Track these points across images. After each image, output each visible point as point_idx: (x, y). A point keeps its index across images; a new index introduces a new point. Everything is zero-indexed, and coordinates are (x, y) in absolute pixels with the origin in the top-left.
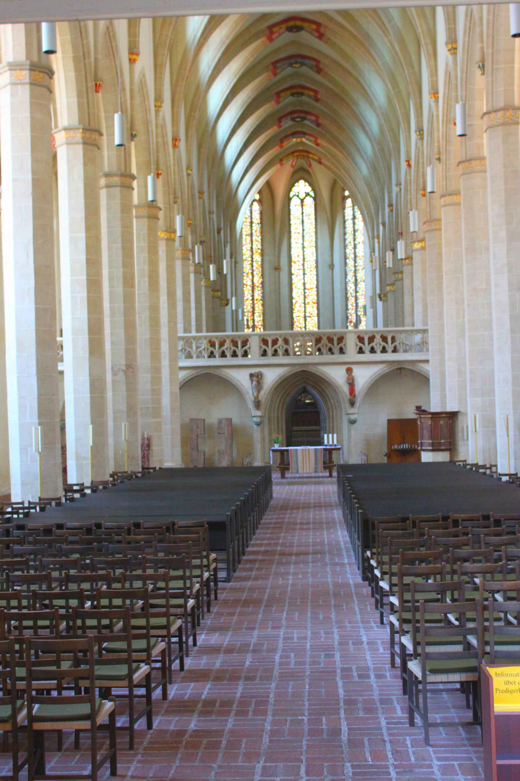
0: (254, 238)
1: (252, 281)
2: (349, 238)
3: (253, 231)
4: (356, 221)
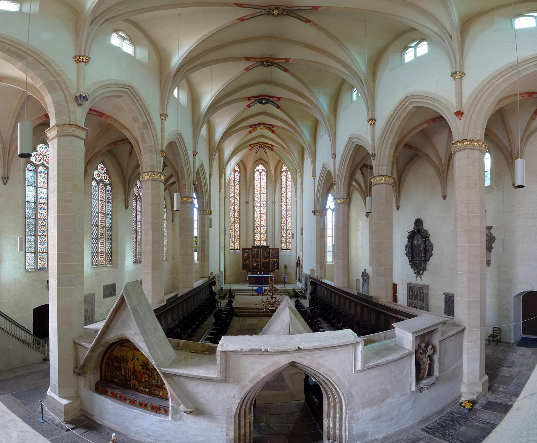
0: (236, 188)
1: (234, 208)
2: (284, 190)
3: (236, 185)
4: (288, 181)
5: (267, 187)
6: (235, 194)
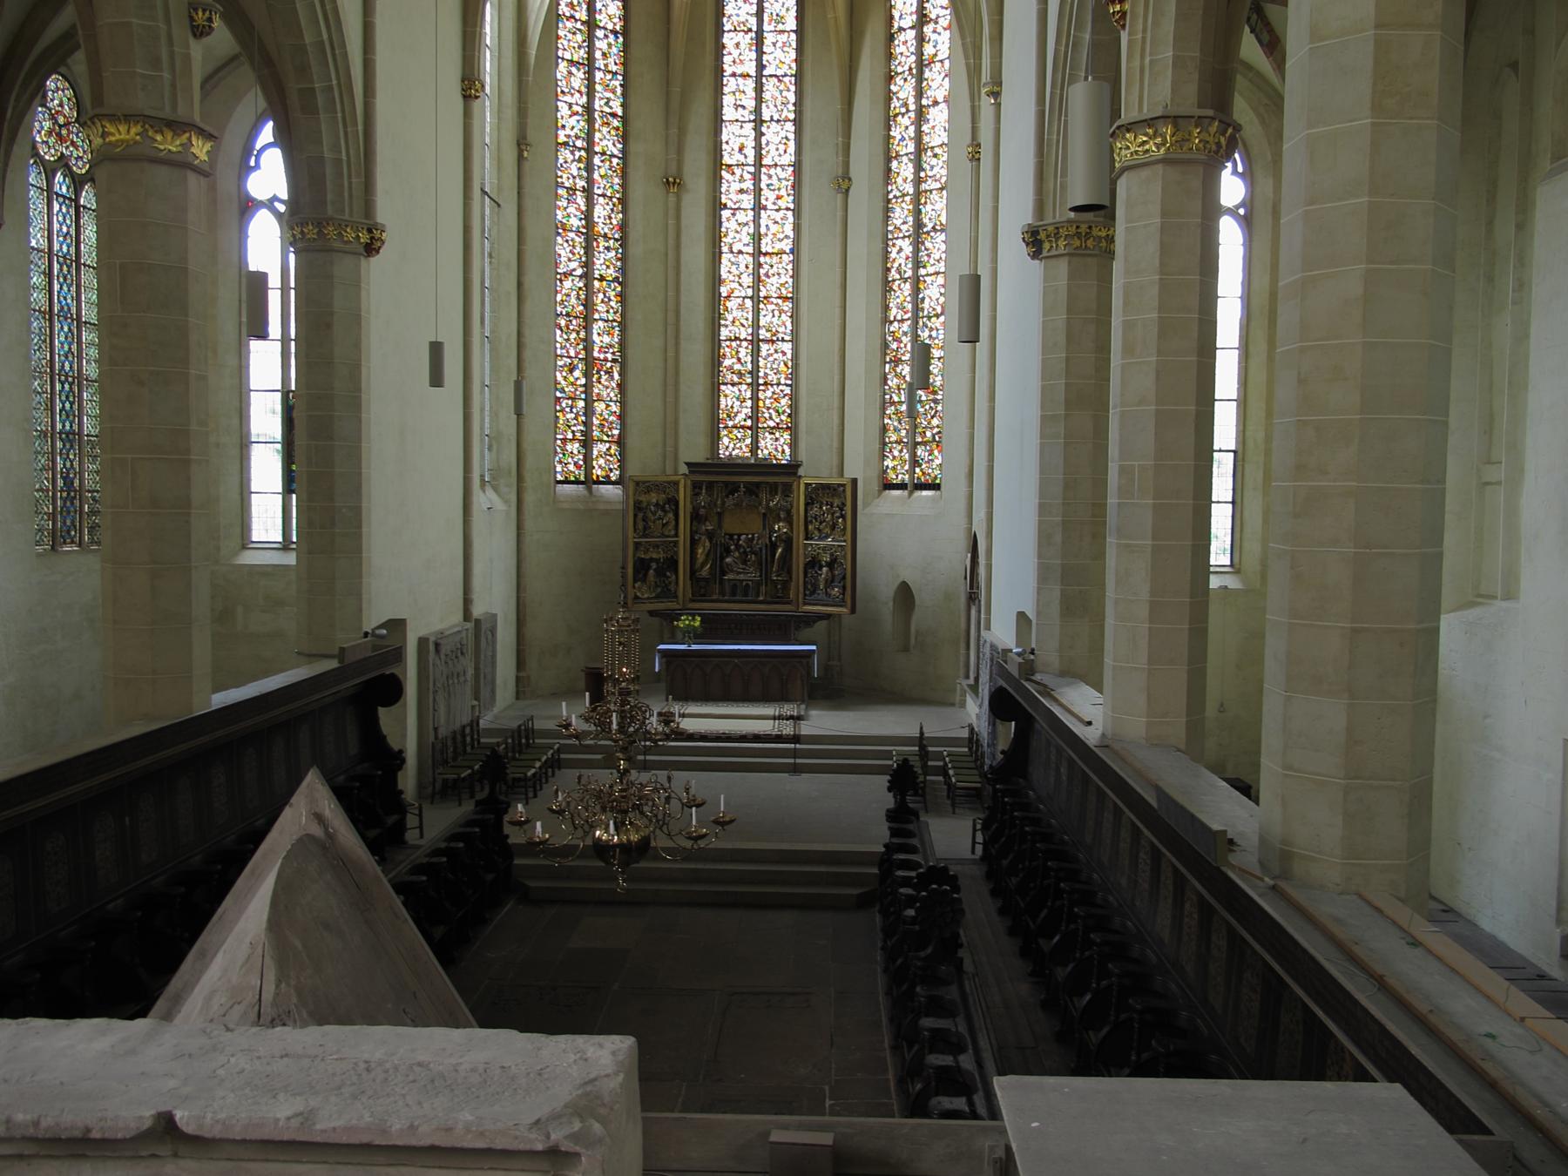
0: (599, 75)
1: (588, 216)
2: (904, 90)
3: (598, 55)
4: (928, 29)
5: (799, 77)
6: (590, 121)
